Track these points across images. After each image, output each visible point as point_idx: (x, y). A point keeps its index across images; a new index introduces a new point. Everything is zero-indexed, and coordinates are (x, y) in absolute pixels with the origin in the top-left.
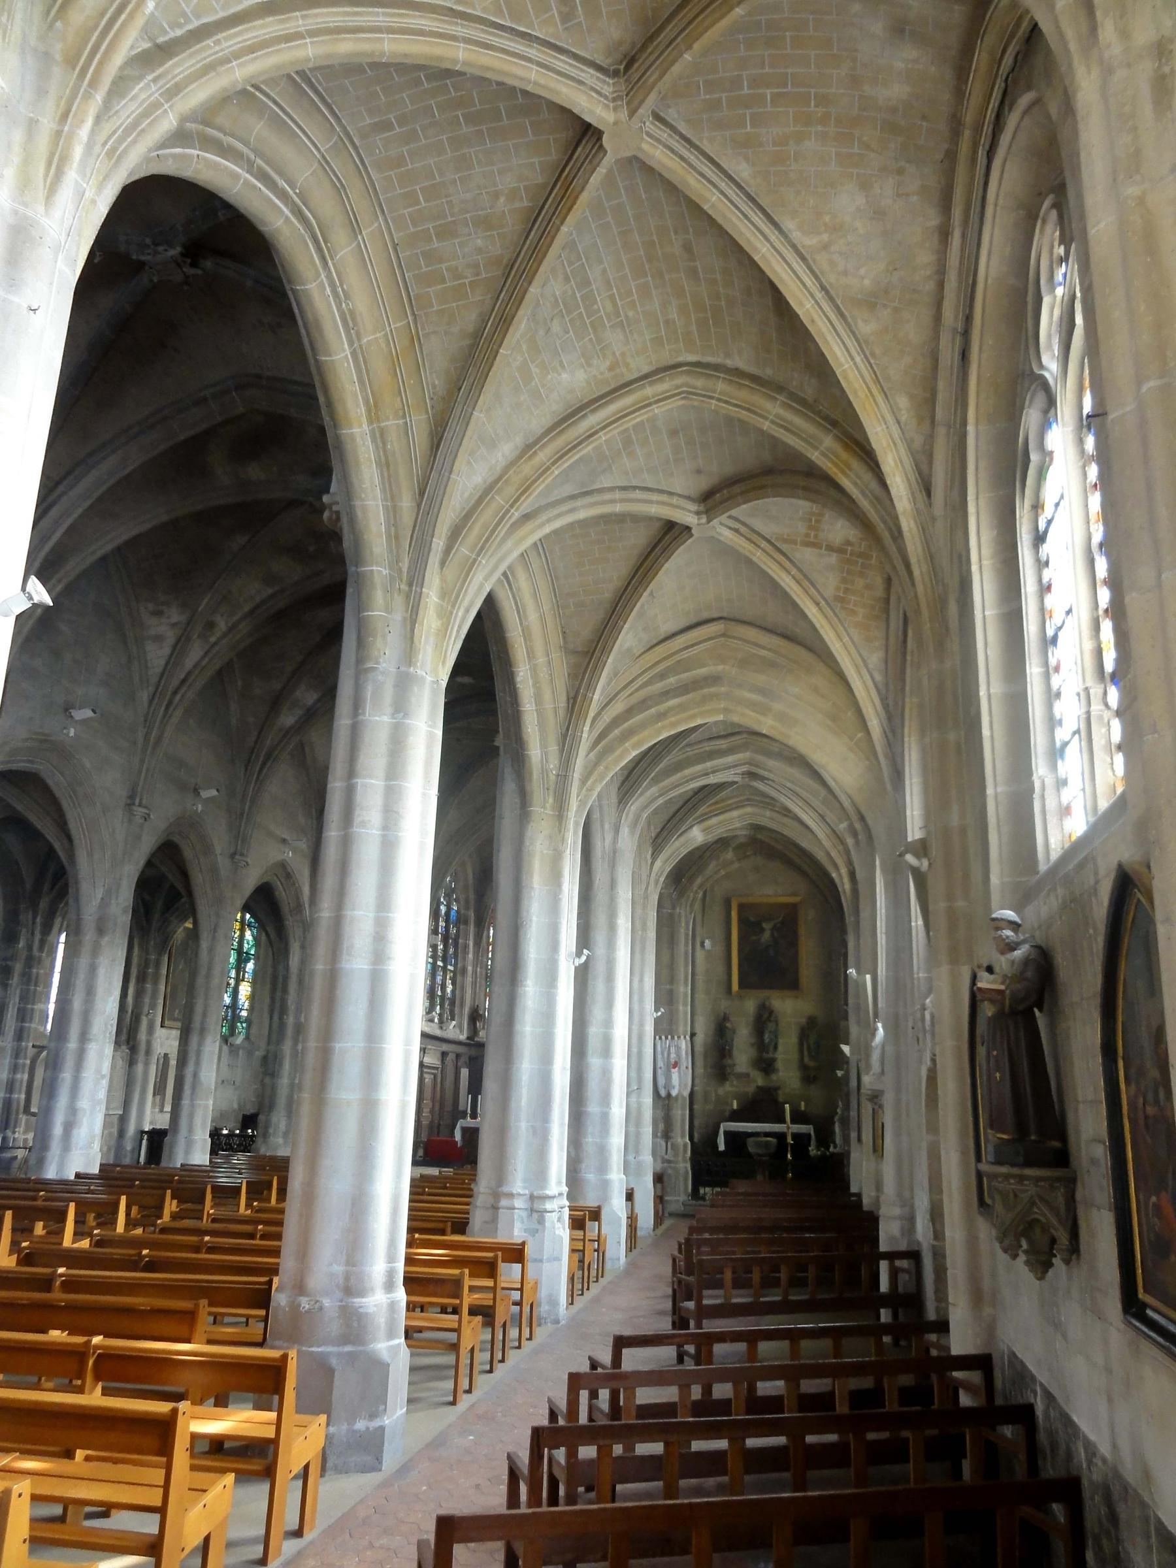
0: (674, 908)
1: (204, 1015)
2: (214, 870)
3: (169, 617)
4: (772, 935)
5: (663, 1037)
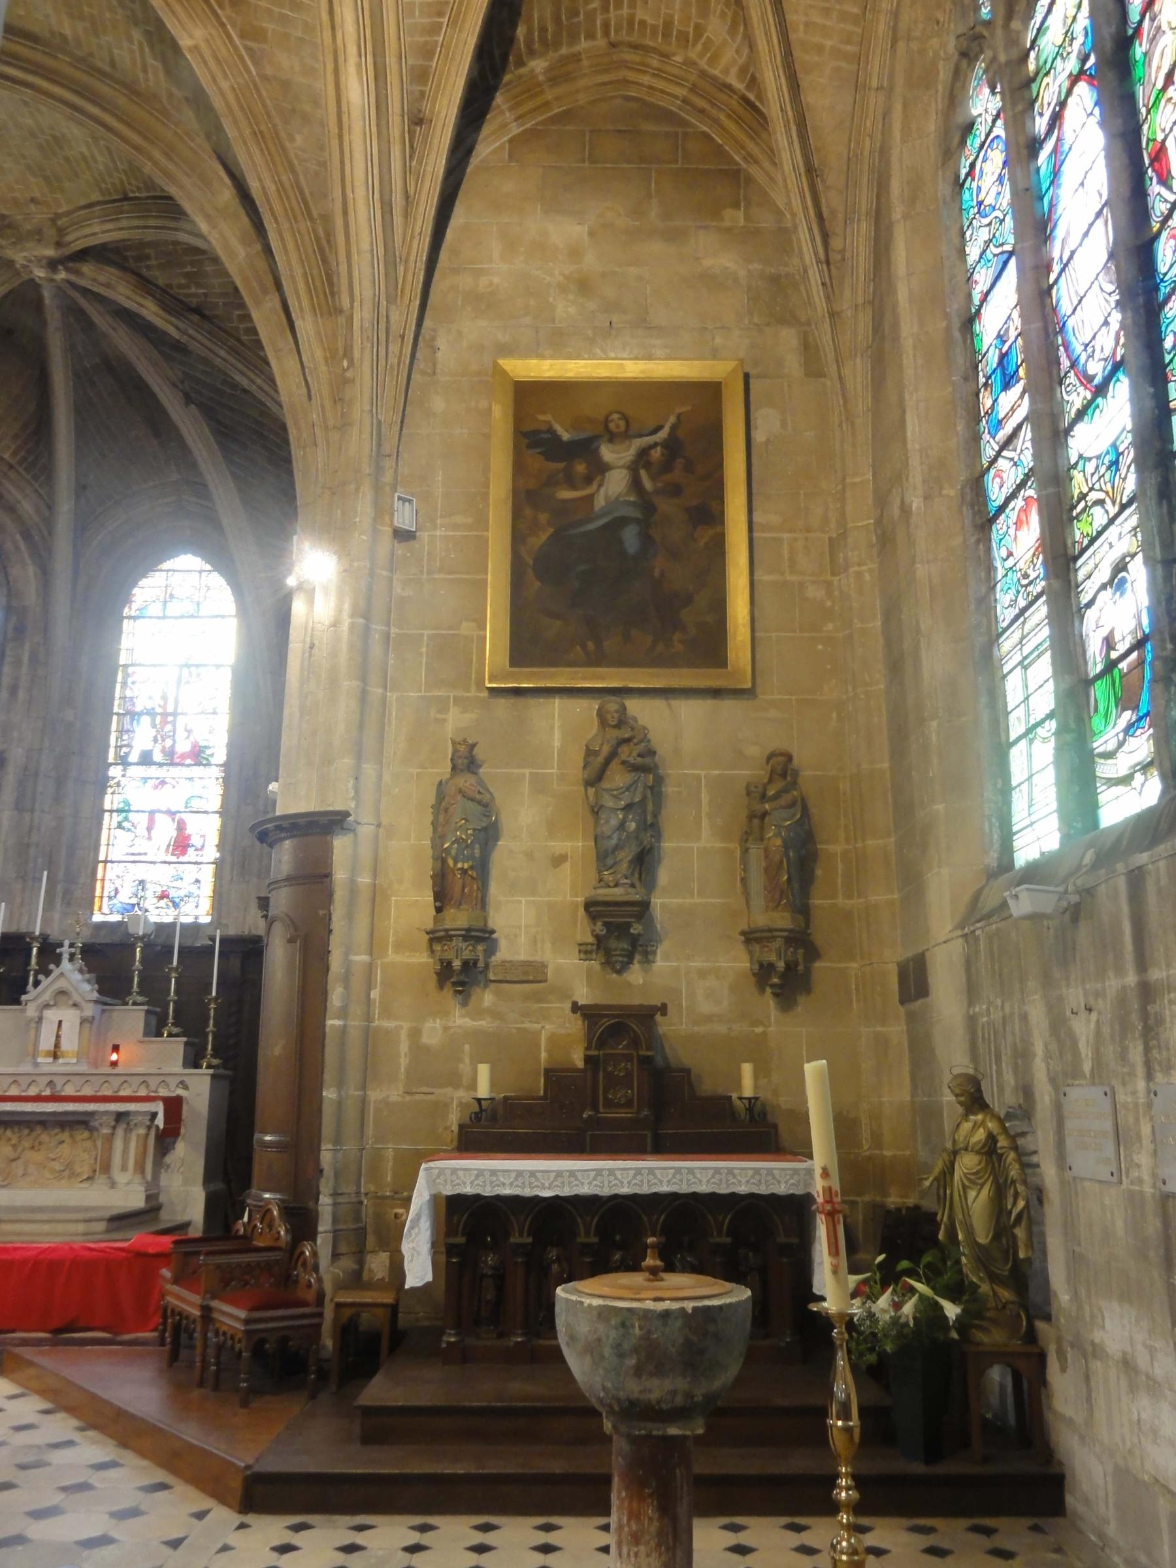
4: (636, 484)
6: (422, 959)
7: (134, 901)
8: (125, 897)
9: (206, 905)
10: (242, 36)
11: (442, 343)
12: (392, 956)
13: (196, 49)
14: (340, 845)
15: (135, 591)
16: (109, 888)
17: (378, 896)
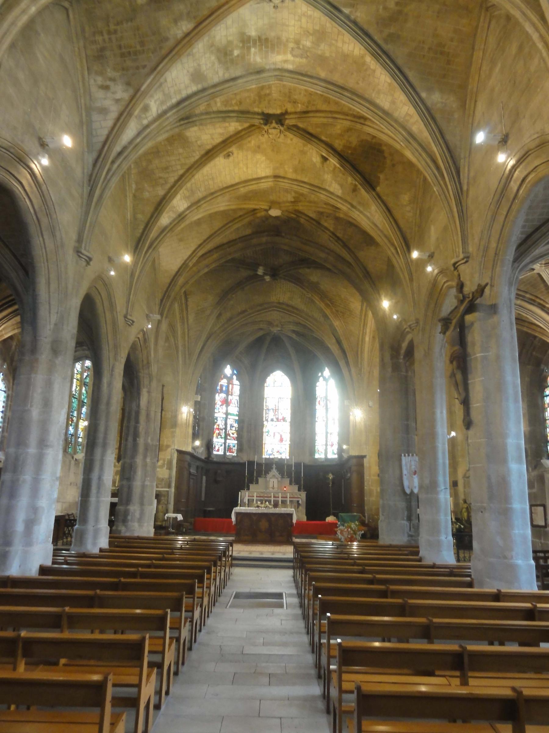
0: (407, 371)
2: (114, 323)
3: (114, 93)
5: (407, 455)
7: (272, 453)
8: (270, 452)
14: (366, 461)
15: (267, 380)
16: (266, 450)
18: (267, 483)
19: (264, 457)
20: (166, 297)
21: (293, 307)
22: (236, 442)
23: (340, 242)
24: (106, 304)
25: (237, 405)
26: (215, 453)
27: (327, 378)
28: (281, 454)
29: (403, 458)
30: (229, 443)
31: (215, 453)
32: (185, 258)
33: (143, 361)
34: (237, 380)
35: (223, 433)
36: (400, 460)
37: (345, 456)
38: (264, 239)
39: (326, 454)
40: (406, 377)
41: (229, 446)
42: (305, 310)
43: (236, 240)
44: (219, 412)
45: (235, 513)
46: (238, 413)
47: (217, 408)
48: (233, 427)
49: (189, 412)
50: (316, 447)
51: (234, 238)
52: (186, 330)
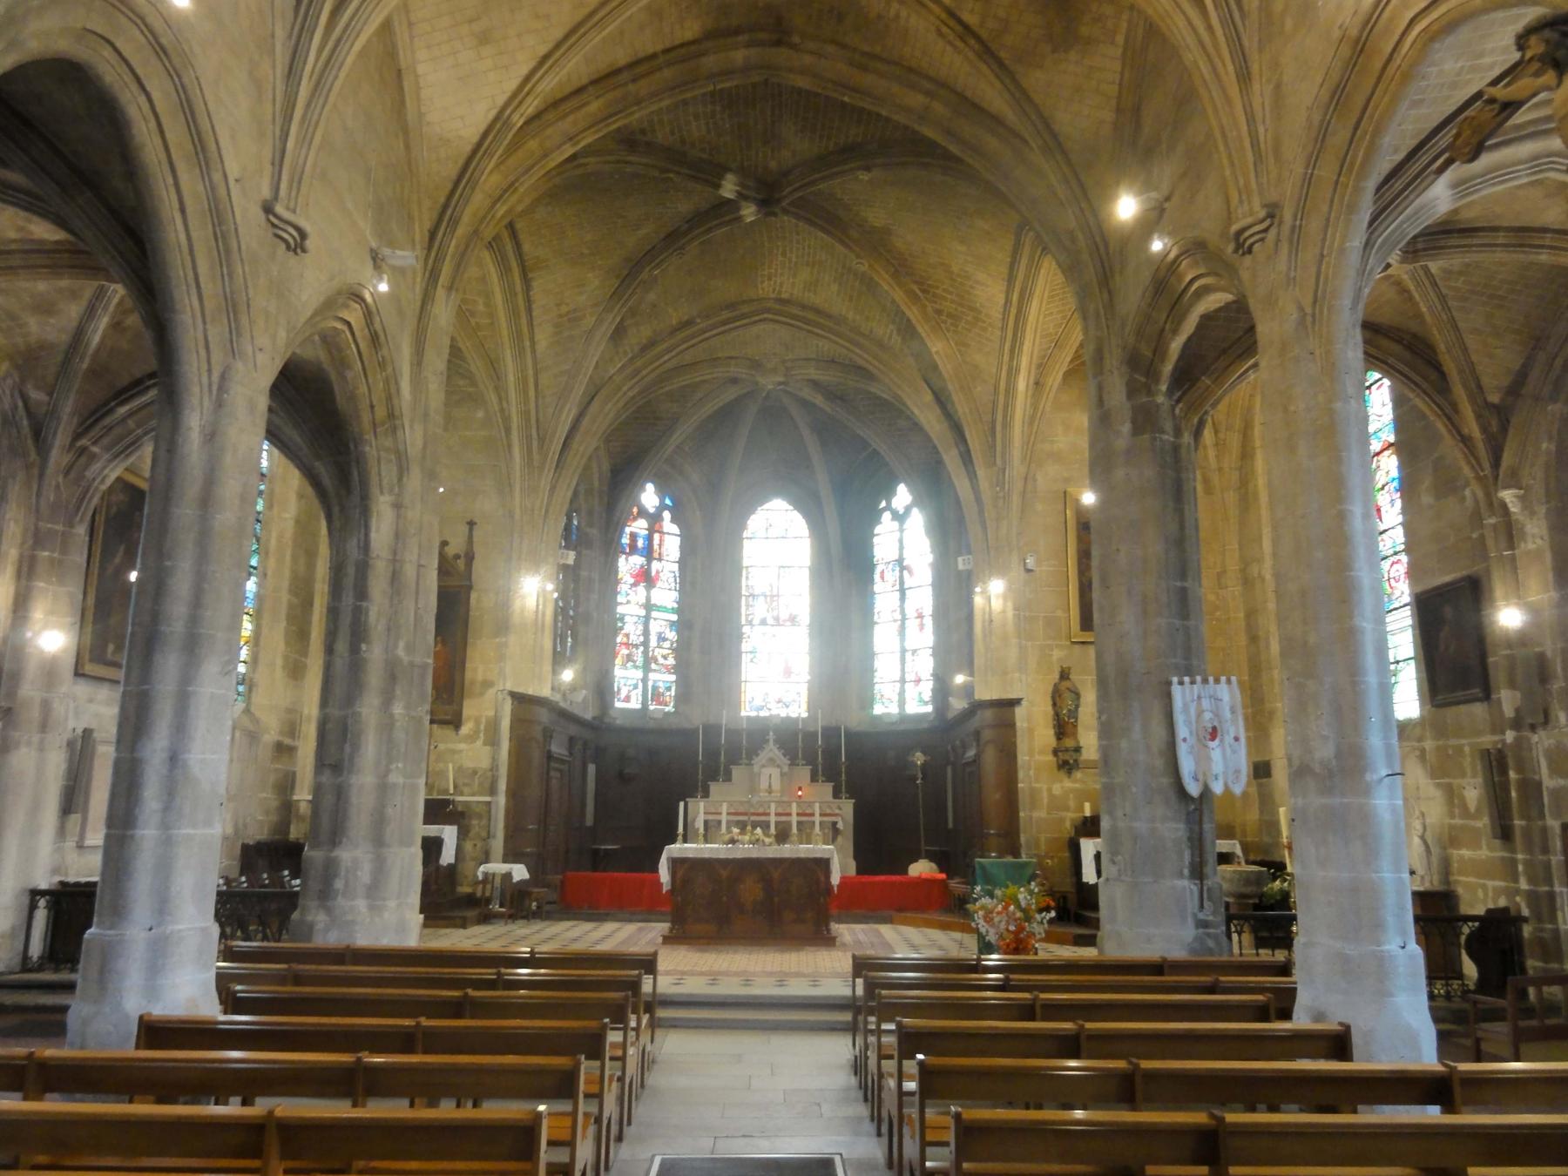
1: (197, 602)
2: (218, 214)
6: (1050, 758)
8: (758, 702)
9: (804, 706)
10: (956, 344)
11: (1039, 477)
12: (1037, 757)
13: (937, 352)
14: (1019, 712)
15: (749, 522)
17: (1031, 731)
18: (753, 780)
19: (743, 714)
20: (444, 224)
21: (818, 311)
22: (673, 678)
23: (972, 42)
24: (176, 133)
25: (673, 585)
26: (618, 705)
27: (901, 511)
28: (787, 707)
29: (1176, 691)
30: (655, 681)
31: (618, 705)
32: (501, 100)
33: (372, 407)
34: (673, 520)
35: (640, 654)
36: (1168, 696)
37: (958, 705)
38: (739, 56)
39: (902, 703)
40: (1176, 449)
41: (655, 688)
42: (850, 315)
43: (654, 56)
44: (628, 602)
45: (668, 859)
46: (676, 606)
47: (623, 592)
48: (665, 639)
49: (543, 593)
50: (877, 687)
51: (650, 51)
52: (531, 372)
